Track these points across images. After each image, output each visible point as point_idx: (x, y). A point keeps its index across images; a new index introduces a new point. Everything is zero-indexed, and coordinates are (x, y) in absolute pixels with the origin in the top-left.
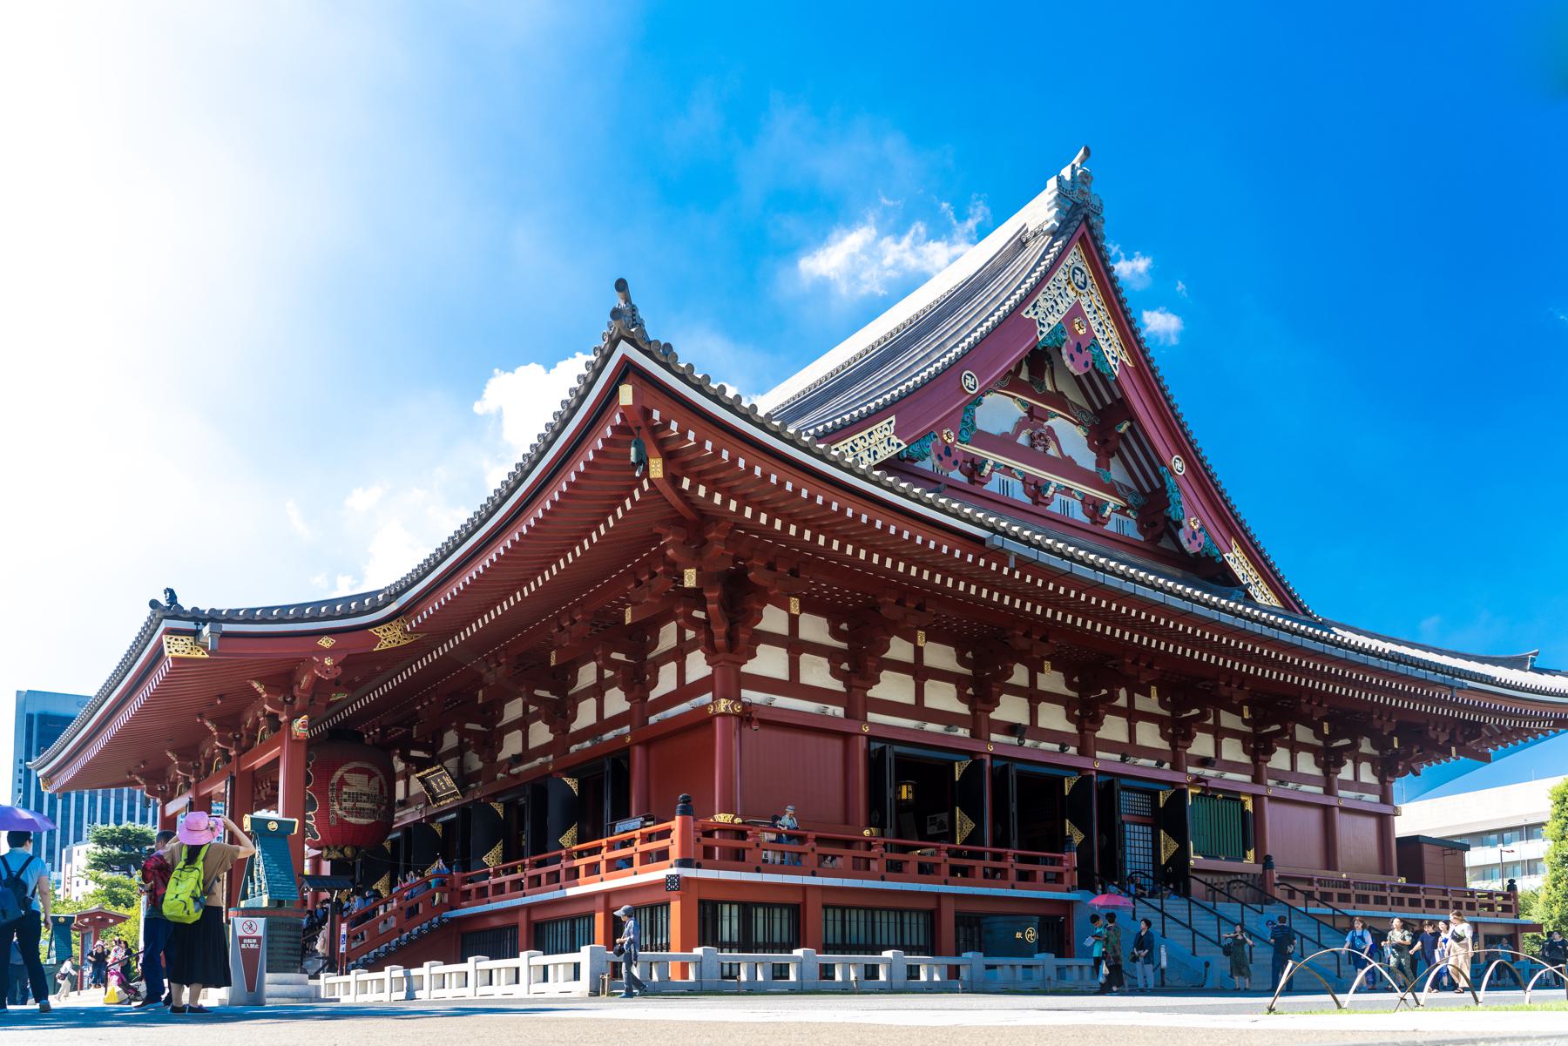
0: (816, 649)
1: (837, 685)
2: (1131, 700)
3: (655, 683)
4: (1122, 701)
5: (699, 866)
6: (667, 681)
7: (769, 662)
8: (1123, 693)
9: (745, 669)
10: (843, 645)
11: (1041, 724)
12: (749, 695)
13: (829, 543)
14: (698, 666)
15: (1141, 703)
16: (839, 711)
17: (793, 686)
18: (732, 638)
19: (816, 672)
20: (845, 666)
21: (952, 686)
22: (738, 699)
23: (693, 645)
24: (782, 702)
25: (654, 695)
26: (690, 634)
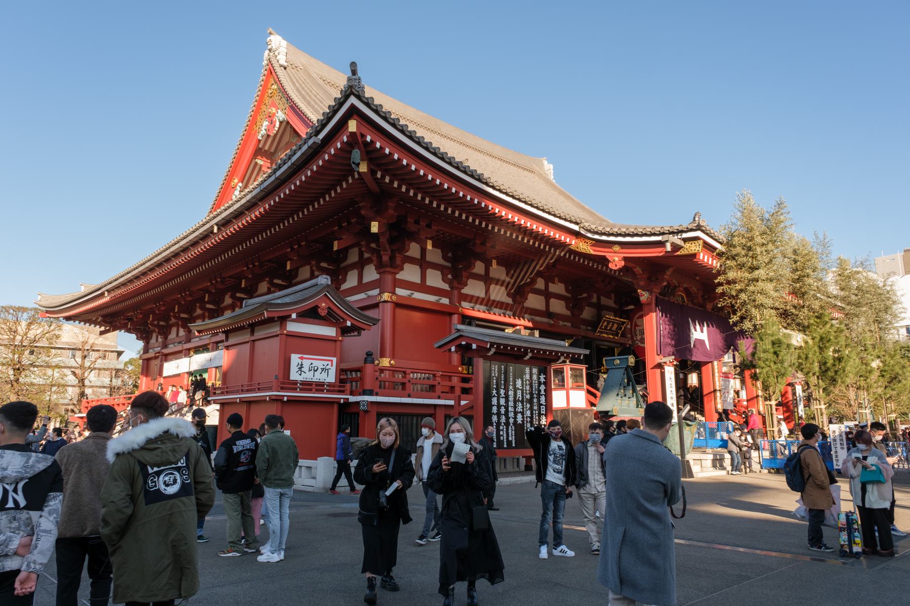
0: (435, 266)
1: (446, 287)
2: (599, 299)
3: (344, 280)
4: (594, 300)
5: (377, 394)
6: (351, 281)
7: (410, 273)
8: (595, 296)
9: (398, 276)
10: (449, 265)
11: (551, 310)
12: (400, 292)
13: (446, 209)
14: (371, 274)
15: (605, 301)
16: (445, 301)
17: (422, 287)
18: (392, 258)
19: (435, 279)
20: (450, 276)
21: (482, 283)
22: (394, 293)
23: (369, 261)
24: (418, 295)
25: (344, 287)
26: (366, 255)
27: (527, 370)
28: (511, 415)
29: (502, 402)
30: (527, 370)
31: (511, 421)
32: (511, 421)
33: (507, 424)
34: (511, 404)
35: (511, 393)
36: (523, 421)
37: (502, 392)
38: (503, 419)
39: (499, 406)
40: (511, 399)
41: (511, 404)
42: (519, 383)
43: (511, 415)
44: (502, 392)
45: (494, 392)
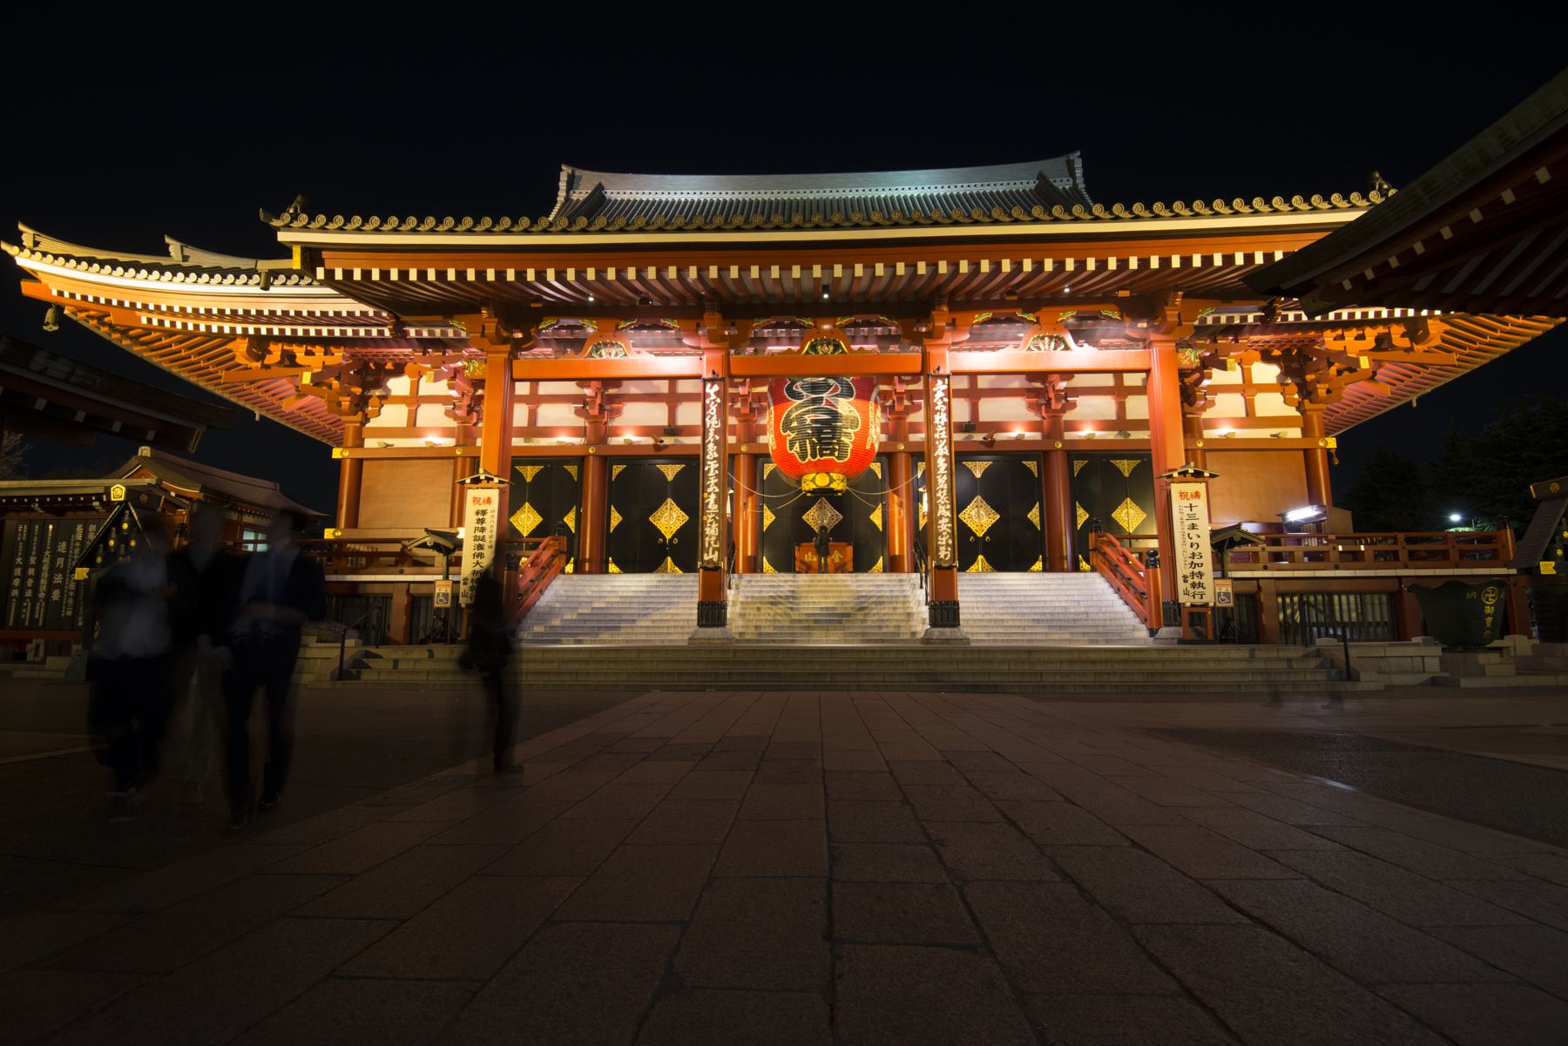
27: (80, 528)
28: (43, 588)
29: (31, 571)
30: (80, 528)
31: (42, 595)
32: (42, 595)
33: (34, 599)
34: (45, 575)
35: (46, 560)
36: (61, 599)
37: (33, 560)
38: (29, 593)
39: (24, 577)
40: (45, 568)
41: (45, 575)
42: (62, 547)
43: (43, 588)
44: (33, 560)
45: (19, 560)
